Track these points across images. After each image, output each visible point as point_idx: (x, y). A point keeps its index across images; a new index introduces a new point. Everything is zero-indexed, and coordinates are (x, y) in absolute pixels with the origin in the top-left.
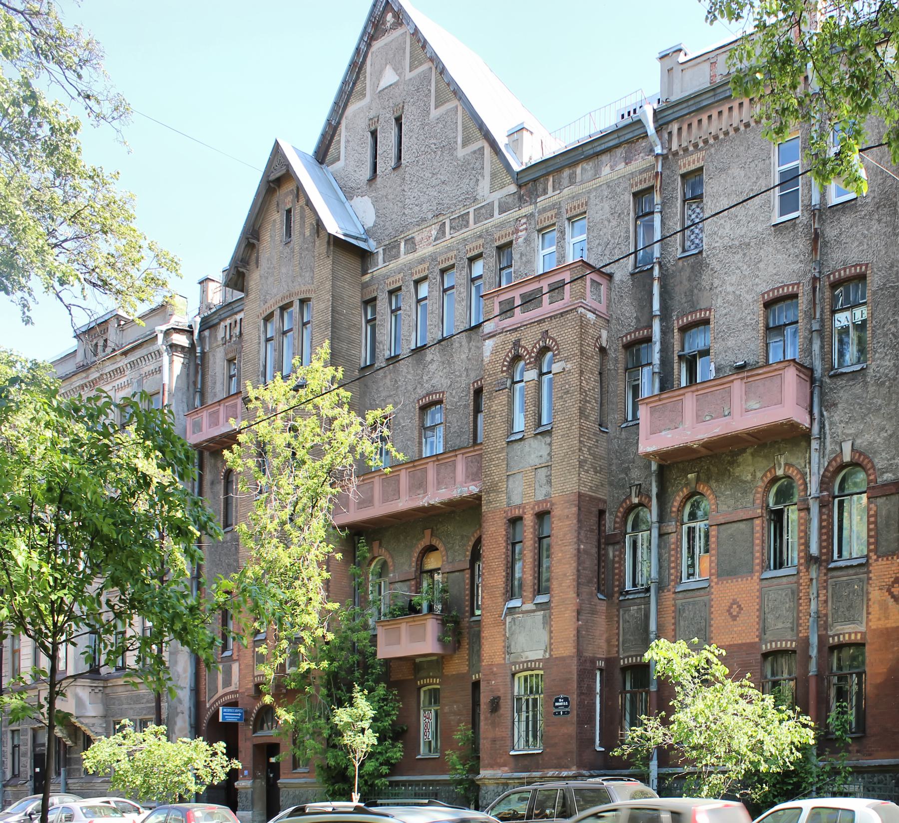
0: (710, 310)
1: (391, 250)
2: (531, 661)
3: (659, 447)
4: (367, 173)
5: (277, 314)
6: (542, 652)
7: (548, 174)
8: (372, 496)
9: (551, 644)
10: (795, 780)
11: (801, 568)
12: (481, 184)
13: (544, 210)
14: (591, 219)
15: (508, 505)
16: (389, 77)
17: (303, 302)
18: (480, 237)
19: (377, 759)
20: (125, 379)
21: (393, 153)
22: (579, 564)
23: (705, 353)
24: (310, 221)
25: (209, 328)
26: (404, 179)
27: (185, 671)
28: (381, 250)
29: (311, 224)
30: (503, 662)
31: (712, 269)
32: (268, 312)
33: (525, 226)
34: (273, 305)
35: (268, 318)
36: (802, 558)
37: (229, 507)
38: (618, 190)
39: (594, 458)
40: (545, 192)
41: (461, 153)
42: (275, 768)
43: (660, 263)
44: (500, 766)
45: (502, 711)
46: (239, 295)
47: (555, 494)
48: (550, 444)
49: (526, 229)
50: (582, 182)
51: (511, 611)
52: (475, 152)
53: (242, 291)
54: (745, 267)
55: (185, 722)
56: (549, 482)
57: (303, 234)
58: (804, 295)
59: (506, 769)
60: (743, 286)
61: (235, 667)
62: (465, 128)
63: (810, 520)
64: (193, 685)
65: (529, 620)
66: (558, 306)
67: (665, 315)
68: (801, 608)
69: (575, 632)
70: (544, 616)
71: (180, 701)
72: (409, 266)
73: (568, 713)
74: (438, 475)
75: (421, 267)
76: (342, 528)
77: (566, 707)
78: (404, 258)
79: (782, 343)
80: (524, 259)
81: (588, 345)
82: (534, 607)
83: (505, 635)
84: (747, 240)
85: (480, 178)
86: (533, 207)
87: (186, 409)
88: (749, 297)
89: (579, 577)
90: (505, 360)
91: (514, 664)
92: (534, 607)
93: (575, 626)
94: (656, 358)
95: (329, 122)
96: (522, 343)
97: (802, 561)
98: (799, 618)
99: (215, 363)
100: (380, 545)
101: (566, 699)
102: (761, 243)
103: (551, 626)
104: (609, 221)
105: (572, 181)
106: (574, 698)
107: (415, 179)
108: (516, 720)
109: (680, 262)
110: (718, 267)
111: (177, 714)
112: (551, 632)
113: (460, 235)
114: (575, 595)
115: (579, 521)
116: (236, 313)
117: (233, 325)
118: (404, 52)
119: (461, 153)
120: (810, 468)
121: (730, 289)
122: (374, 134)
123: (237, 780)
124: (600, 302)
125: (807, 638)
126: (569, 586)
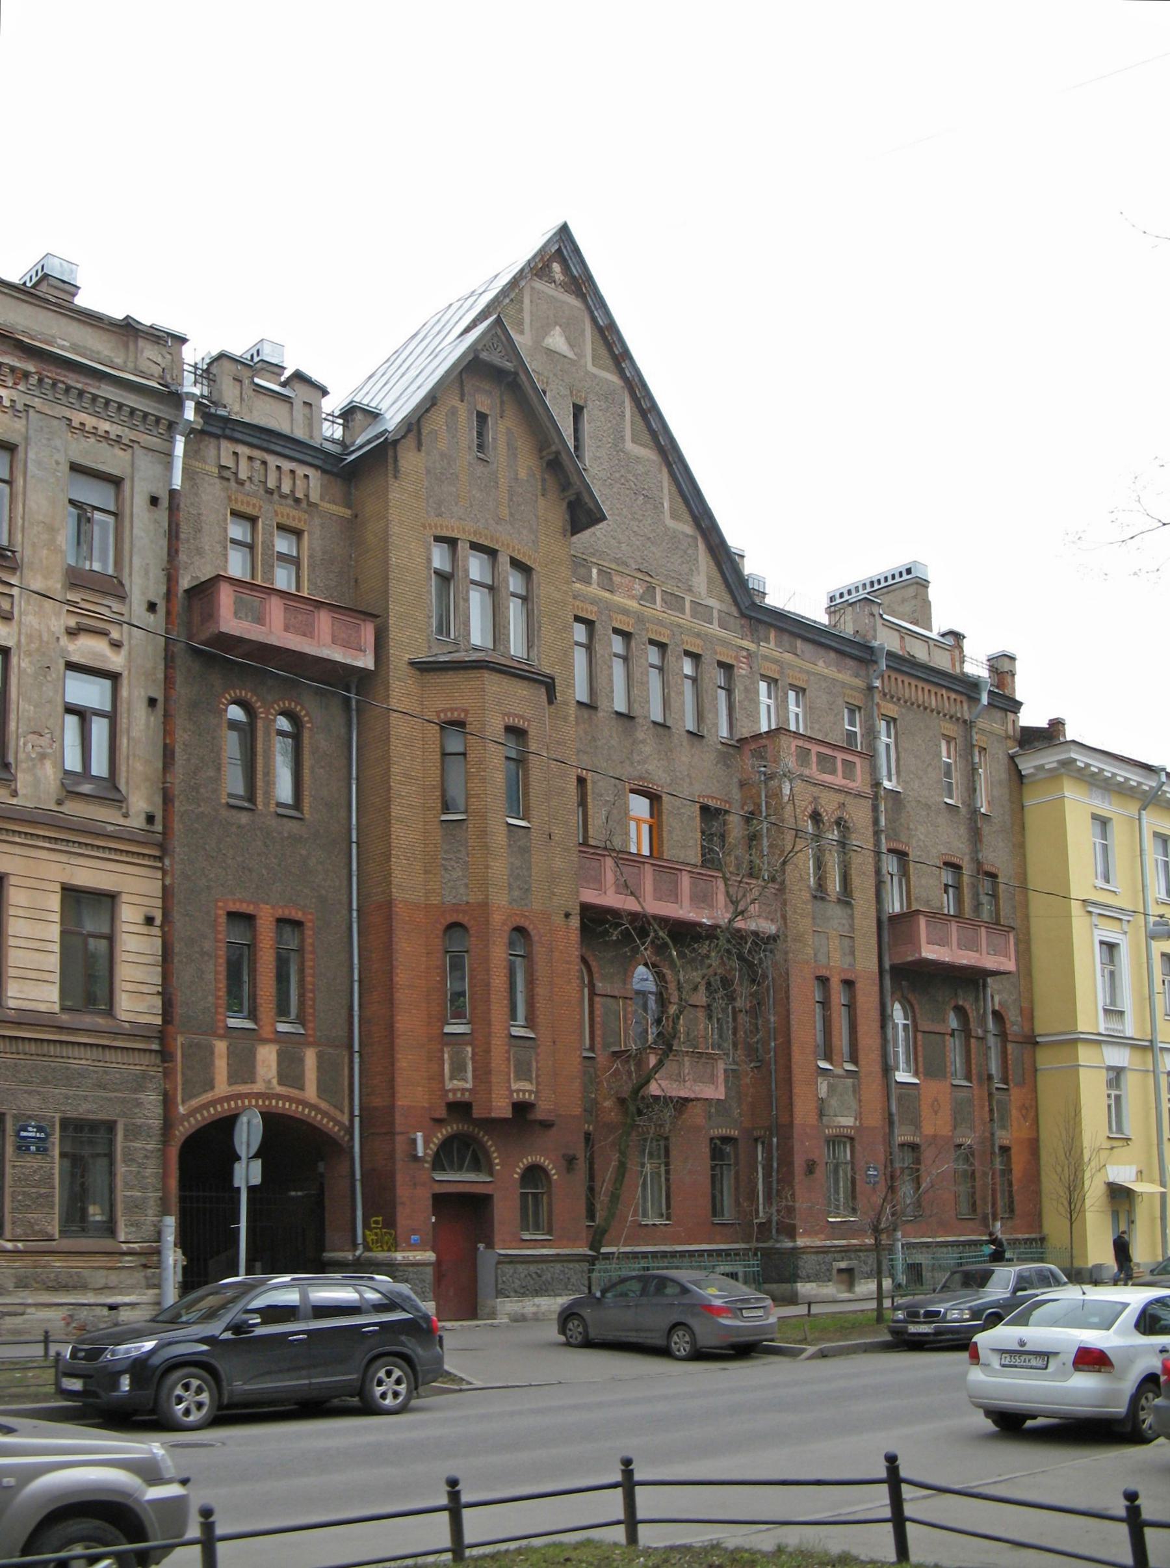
2: (844, 1127)
7: (771, 625)
18: (698, 635)
44: (816, 1233)
70: (854, 1086)
91: (828, 1127)
112: (860, 1101)
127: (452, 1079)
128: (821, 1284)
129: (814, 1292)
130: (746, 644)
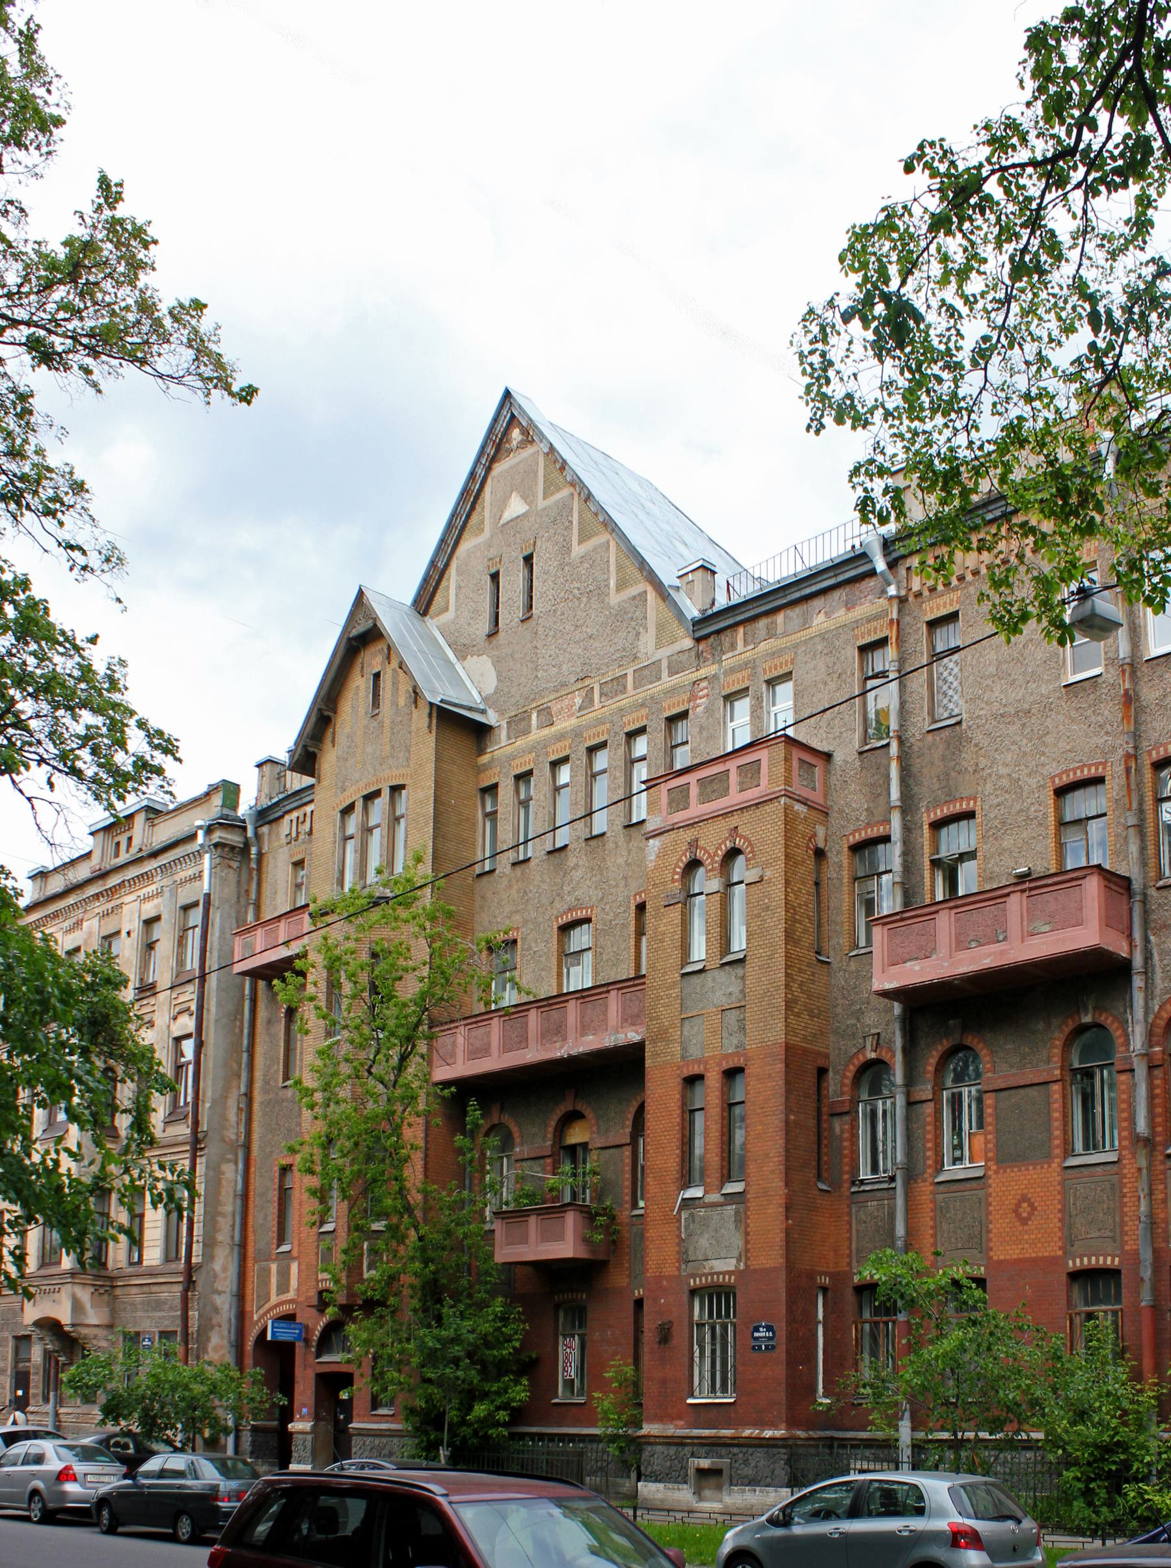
0: (975, 799)
1: (519, 724)
2: (718, 1274)
3: (902, 984)
4: (485, 626)
5: (359, 806)
6: (734, 1261)
8: (489, 1044)
9: (747, 1250)
10: (1122, 1457)
11: (1124, 1153)
12: (644, 638)
13: (732, 670)
14: (799, 681)
15: (683, 1057)
16: (516, 507)
17: (396, 789)
18: (643, 705)
19: (492, 1402)
20: (153, 887)
21: (520, 601)
22: (787, 1141)
23: (970, 855)
24: (405, 688)
25: (270, 822)
26: (536, 633)
27: (225, 1269)
28: (504, 724)
29: (407, 691)
30: (677, 1273)
31: (976, 745)
32: (348, 802)
33: (705, 691)
34: (354, 794)
35: (348, 810)
36: (1125, 1138)
37: (291, 1053)
38: (837, 643)
39: (810, 997)
40: (733, 646)
41: (614, 599)
42: (347, 1407)
43: (899, 738)
44: (671, 1418)
45: (674, 1342)
46: (308, 781)
47: (751, 1045)
48: (743, 978)
49: (708, 695)
50: (786, 634)
51: (688, 1203)
52: (634, 598)
53: (313, 776)
54: (1025, 741)
55: (222, 1338)
56: (742, 1029)
57: (395, 704)
58: (1113, 778)
59: (682, 1423)
60: (1022, 767)
61: (294, 1267)
62: (620, 568)
63: (1135, 1085)
64: (235, 1289)
65: (715, 1214)
66: (752, 794)
67: (908, 806)
68: (1126, 1209)
69: (783, 1235)
70: (737, 1213)
71: (216, 1310)
72: (544, 744)
73: (773, 1347)
74: (582, 1017)
75: (559, 745)
76: (446, 1084)
77: (769, 1338)
78: (537, 734)
79: (1084, 842)
80: (705, 734)
81: (797, 846)
82: (722, 1199)
83: (679, 1236)
84: (1026, 706)
85: (641, 630)
86: (716, 667)
87: (234, 925)
88: (1033, 782)
89: (787, 1158)
90: (677, 866)
91: (694, 1276)
92: (722, 1199)
93: (784, 1226)
94: (897, 863)
95: (433, 564)
96: (701, 843)
97: (1125, 1143)
98: (1123, 1224)
99: (276, 867)
100: (502, 1110)
101: (769, 1328)
102: (1047, 708)
103: (747, 1226)
104: (825, 684)
105: (771, 634)
106: (782, 1328)
107: (552, 633)
108: (697, 1354)
109: (930, 737)
110: (985, 743)
111: (212, 1327)
112: (747, 1234)
113: (614, 704)
114: (782, 1184)
115: (787, 1082)
116: (306, 804)
117: (301, 819)
118: (536, 476)
119: (614, 599)
120: (1132, 1014)
121: (1003, 771)
122: (495, 577)
123: (292, 1421)
124: (814, 789)
125: (1136, 1253)
126: (773, 1172)
127: (369, 1269)
128: (670, 1486)
129: (659, 1496)
130: (702, 673)
